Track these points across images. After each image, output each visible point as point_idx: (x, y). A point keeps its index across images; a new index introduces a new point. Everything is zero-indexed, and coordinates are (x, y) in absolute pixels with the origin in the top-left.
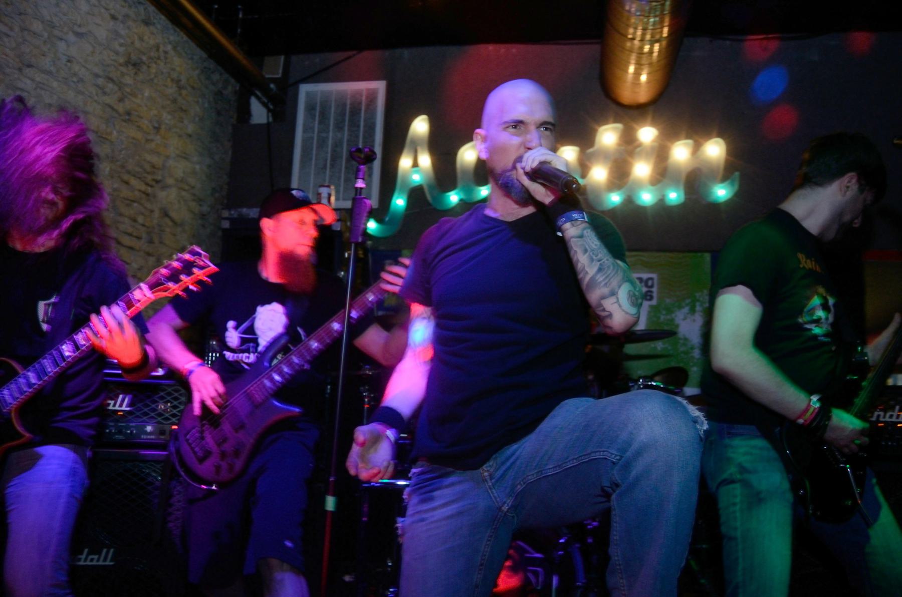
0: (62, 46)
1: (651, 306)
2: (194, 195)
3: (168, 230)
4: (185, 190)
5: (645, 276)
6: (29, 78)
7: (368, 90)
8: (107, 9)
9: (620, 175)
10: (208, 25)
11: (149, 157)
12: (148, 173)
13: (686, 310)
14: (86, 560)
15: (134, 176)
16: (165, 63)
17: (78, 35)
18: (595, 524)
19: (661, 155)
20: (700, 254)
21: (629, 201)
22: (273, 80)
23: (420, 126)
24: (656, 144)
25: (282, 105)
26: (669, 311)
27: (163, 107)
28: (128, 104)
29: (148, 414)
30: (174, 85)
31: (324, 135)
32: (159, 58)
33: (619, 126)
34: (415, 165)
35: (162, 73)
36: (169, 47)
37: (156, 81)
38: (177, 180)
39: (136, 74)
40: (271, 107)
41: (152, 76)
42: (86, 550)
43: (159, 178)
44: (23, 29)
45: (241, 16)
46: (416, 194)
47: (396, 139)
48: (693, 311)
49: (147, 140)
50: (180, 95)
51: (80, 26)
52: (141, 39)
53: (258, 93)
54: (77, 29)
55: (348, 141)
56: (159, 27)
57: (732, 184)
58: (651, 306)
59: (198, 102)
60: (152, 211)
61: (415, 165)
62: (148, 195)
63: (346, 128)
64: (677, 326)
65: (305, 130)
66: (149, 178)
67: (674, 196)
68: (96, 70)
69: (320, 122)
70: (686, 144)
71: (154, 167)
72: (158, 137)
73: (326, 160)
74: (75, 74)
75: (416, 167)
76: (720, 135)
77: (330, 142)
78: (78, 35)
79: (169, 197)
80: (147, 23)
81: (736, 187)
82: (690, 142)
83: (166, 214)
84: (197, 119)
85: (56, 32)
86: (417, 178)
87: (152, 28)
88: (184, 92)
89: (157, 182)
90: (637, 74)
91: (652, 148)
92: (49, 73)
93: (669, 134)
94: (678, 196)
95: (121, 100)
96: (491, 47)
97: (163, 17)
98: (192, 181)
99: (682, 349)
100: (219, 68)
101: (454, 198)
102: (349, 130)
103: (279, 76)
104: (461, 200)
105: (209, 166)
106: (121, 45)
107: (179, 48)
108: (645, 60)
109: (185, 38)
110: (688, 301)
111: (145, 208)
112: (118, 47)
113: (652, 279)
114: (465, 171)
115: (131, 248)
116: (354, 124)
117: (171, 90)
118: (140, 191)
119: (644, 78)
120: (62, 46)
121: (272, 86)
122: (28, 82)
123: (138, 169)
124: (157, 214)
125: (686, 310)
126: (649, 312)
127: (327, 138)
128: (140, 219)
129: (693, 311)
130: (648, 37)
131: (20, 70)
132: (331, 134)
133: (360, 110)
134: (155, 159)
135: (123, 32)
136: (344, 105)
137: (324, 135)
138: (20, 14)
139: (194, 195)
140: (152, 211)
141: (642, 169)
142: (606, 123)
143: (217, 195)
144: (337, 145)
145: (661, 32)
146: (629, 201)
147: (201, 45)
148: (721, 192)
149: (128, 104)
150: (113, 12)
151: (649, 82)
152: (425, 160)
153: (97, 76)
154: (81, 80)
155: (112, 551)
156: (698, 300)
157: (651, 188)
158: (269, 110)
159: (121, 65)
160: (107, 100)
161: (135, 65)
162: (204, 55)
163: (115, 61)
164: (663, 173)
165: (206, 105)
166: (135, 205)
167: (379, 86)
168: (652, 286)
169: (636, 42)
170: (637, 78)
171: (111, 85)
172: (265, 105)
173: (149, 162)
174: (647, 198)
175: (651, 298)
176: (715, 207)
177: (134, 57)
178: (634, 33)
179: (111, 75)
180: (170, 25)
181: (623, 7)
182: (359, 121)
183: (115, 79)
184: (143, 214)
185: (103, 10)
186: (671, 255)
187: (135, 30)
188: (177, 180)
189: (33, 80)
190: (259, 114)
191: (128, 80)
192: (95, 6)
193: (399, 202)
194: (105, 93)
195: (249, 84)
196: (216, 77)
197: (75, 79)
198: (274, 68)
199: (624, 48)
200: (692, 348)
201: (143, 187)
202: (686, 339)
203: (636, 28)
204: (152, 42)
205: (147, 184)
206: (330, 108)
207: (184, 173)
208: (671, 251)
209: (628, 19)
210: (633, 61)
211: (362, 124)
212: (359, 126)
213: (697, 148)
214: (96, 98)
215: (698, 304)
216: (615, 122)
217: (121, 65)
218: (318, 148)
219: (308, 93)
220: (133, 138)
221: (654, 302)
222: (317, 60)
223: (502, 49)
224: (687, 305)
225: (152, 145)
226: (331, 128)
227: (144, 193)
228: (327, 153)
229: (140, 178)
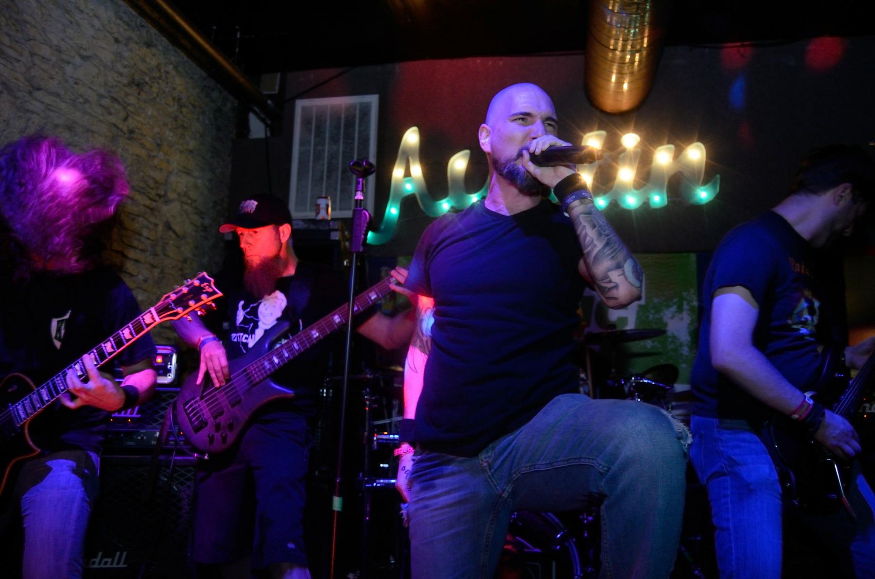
0: (69, 69)
1: (640, 306)
2: (197, 208)
3: (171, 242)
4: (186, 204)
6: (39, 101)
7: (361, 104)
8: (111, 33)
9: (605, 180)
10: (206, 46)
11: (152, 174)
12: (152, 189)
14: (100, 563)
15: (138, 191)
16: (167, 83)
17: (84, 58)
18: (590, 518)
19: (644, 159)
20: (685, 255)
21: (614, 205)
22: (270, 97)
23: (411, 137)
24: (639, 150)
25: (279, 120)
26: (658, 310)
27: (165, 124)
28: (131, 123)
29: (157, 421)
30: (176, 104)
31: (320, 148)
32: (160, 78)
33: (603, 133)
34: (408, 174)
35: (164, 92)
36: (171, 67)
37: (158, 100)
38: (179, 194)
39: (139, 94)
40: (269, 122)
41: (155, 95)
42: (100, 554)
43: (162, 193)
44: (32, 54)
45: (238, 36)
46: (409, 203)
47: (390, 149)
48: (680, 309)
49: (149, 156)
50: (181, 112)
51: (85, 50)
52: (143, 60)
53: (256, 109)
54: (83, 52)
55: (344, 152)
56: (160, 48)
59: (198, 119)
60: (156, 225)
61: (408, 174)
62: (152, 209)
63: (341, 140)
64: (666, 325)
65: (302, 144)
66: (153, 193)
67: (658, 200)
68: (102, 91)
69: (316, 136)
70: (669, 149)
71: (156, 182)
72: (161, 154)
73: (323, 173)
74: (81, 96)
75: (408, 177)
76: (700, 140)
77: (326, 155)
78: (84, 58)
79: (172, 211)
80: (149, 45)
81: (718, 190)
82: (672, 146)
83: (168, 227)
84: (198, 135)
85: (64, 57)
86: (409, 188)
87: (154, 50)
88: (184, 110)
89: (160, 196)
90: (619, 83)
91: (635, 153)
92: (58, 95)
93: (651, 140)
94: (662, 199)
95: (126, 119)
96: (479, 60)
97: (164, 39)
98: (193, 195)
99: (671, 347)
100: (219, 86)
101: (445, 206)
102: (344, 143)
103: (276, 92)
104: (452, 207)
105: (210, 180)
106: (125, 67)
107: (180, 69)
108: (626, 70)
109: (186, 58)
110: (675, 300)
111: (150, 222)
112: (121, 70)
114: (455, 180)
115: (137, 261)
116: (349, 137)
117: (173, 109)
118: (144, 205)
119: (626, 86)
120: (69, 69)
121: (269, 102)
122: (38, 104)
123: (142, 185)
124: (160, 228)
125: (674, 309)
126: (638, 312)
127: (324, 150)
128: (145, 233)
129: (680, 309)
130: (629, 47)
131: (30, 93)
132: (327, 146)
133: (354, 123)
134: (157, 175)
135: (126, 54)
136: (340, 118)
137: (320, 148)
138: (30, 40)
139: (197, 208)
140: (156, 225)
141: (626, 174)
142: (591, 130)
143: (219, 208)
144: (333, 157)
145: (642, 42)
146: (614, 205)
147: (201, 65)
148: (704, 195)
149: (131, 123)
150: (116, 35)
151: (630, 90)
152: (417, 170)
153: (101, 96)
154: (87, 101)
155: (125, 554)
156: (686, 299)
157: (635, 191)
158: (267, 125)
159: (124, 86)
160: (112, 119)
161: (138, 85)
162: (204, 74)
163: (119, 82)
164: (647, 177)
165: (207, 122)
166: (141, 219)
167: (373, 100)
169: (618, 53)
170: (620, 87)
171: (116, 106)
172: (263, 120)
173: (153, 178)
174: (631, 201)
176: (698, 208)
177: (137, 77)
178: (616, 44)
179: (115, 96)
180: (171, 47)
181: (605, 19)
182: (354, 134)
183: (120, 100)
184: (148, 228)
185: (107, 34)
186: (657, 256)
187: (138, 52)
188: (179, 194)
189: (42, 103)
190: (257, 129)
191: (132, 100)
192: (99, 30)
193: (393, 211)
194: (110, 114)
195: (247, 102)
196: (215, 94)
197: (81, 100)
198: (271, 85)
199: (607, 59)
201: (148, 202)
202: (674, 337)
203: (617, 40)
204: (154, 63)
205: (150, 199)
206: (326, 121)
207: (187, 187)
208: (659, 252)
209: (610, 31)
210: (615, 71)
211: (356, 136)
212: (353, 139)
213: (678, 153)
214: (101, 118)
215: (685, 303)
216: (599, 129)
217: (124, 86)
218: (314, 162)
219: (304, 109)
220: (137, 155)
221: (642, 302)
222: (314, 76)
223: (490, 62)
224: (674, 304)
225: (156, 162)
226: (327, 141)
227: (147, 207)
228: (323, 165)
229: (144, 194)
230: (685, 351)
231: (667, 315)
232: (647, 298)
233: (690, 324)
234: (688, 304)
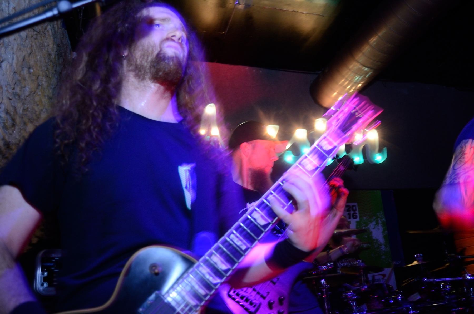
1: (357, 222)
5: (351, 204)
13: (374, 223)
48: (377, 224)
57: (383, 154)
58: (357, 222)
64: (371, 233)
113: (355, 206)
125: (374, 223)
168: (355, 210)
175: (356, 218)
176: (376, 166)
200: (381, 245)
202: (377, 240)
215: (379, 219)
221: (358, 219)
230: (383, 248)
231: (371, 226)
232: (360, 217)
233: (383, 232)
234: (381, 220)
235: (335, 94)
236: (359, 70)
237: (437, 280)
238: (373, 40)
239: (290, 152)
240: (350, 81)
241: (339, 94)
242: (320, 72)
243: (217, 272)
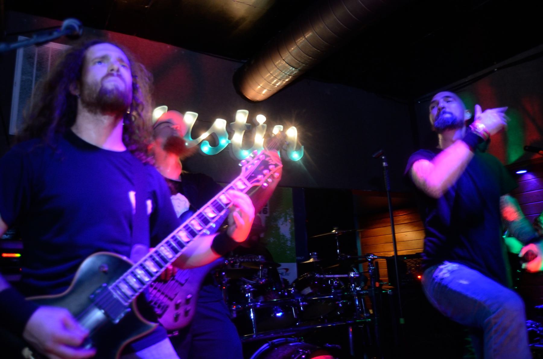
1: (267, 217)
13: (283, 219)
24: (265, 125)
33: (247, 112)
48: (286, 220)
64: (279, 228)
69: (37, 70)
91: (263, 126)
96: (169, 47)
110: (283, 214)
125: (283, 219)
129: (286, 220)
200: (287, 241)
202: (284, 236)
215: (288, 216)
221: (268, 215)
230: (289, 243)
233: (291, 228)
235: (259, 87)
236: (285, 68)
237: (327, 276)
238: (301, 41)
239: (207, 142)
240: (276, 77)
241: (263, 88)
242: (246, 61)
243: (149, 273)
